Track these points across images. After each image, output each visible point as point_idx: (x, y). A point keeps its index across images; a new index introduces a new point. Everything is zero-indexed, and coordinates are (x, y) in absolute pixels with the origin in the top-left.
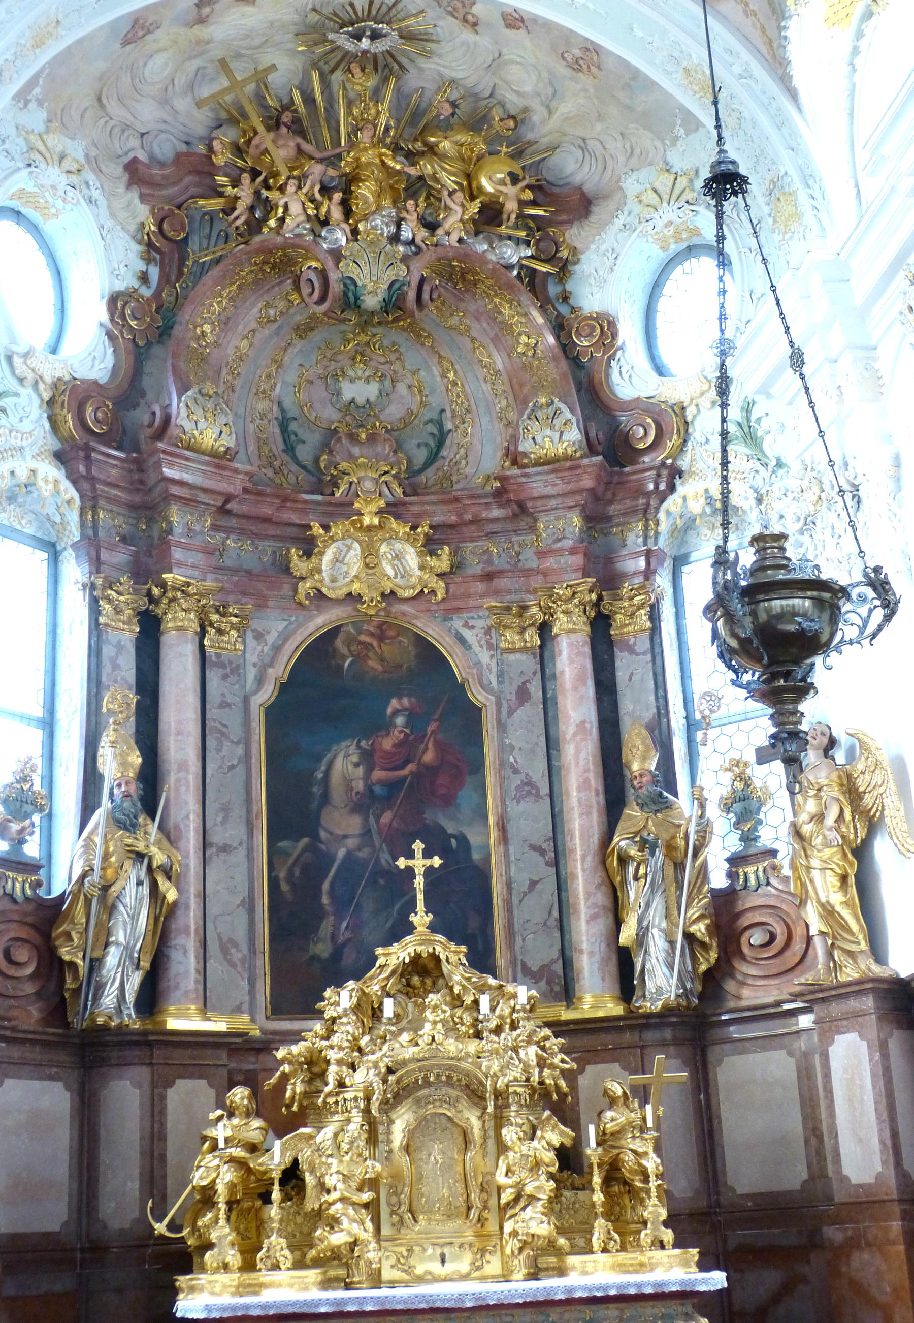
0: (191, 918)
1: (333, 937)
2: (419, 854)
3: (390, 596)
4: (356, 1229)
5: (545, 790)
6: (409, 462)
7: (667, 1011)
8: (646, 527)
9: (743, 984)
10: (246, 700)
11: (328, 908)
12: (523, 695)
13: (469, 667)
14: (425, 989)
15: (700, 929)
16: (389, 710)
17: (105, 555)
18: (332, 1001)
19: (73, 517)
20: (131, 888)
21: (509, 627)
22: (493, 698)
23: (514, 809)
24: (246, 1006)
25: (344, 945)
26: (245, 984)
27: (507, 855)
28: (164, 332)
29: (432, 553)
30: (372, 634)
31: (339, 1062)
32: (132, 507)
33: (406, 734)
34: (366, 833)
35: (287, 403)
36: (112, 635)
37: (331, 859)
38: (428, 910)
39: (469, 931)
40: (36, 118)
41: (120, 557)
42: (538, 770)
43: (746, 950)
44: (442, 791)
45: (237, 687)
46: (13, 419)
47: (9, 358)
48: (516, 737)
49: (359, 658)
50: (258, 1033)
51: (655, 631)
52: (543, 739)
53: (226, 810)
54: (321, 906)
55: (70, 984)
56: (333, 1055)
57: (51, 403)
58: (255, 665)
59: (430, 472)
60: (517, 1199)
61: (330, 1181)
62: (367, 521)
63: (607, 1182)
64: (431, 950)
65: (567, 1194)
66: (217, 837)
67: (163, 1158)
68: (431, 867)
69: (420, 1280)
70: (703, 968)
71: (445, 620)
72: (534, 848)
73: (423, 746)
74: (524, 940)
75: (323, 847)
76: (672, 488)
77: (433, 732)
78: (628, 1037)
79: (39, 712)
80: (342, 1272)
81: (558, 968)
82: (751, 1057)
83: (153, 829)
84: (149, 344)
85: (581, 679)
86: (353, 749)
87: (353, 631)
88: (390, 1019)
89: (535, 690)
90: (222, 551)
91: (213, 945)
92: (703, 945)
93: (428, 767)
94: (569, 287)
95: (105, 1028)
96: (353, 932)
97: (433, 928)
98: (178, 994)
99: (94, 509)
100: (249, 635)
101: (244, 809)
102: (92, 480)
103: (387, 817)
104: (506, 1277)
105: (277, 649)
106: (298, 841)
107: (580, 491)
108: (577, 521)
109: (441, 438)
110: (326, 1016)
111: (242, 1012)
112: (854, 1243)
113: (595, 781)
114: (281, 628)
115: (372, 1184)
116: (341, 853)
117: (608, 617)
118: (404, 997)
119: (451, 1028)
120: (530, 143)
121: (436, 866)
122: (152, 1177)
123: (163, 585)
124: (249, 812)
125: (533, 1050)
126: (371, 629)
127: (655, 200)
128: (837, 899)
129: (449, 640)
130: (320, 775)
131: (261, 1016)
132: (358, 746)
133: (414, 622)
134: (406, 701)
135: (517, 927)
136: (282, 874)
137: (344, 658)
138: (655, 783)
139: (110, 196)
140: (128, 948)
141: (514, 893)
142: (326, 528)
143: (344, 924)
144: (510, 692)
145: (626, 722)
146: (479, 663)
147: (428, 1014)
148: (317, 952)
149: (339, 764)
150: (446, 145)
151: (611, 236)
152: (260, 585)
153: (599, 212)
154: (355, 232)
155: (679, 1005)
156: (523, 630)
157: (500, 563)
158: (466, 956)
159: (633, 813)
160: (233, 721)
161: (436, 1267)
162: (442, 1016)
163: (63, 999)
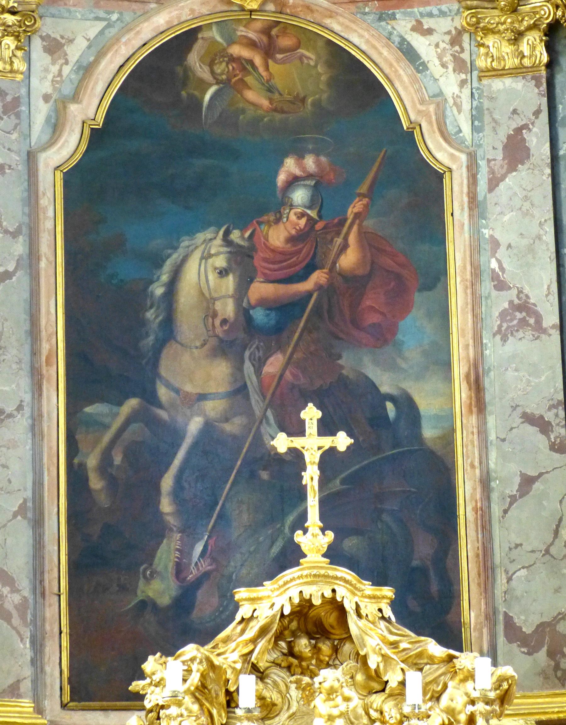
2: (312, 428)
11: (171, 520)
13: (422, 102)
14: (319, 661)
16: (282, 178)
18: (156, 678)
21: (493, 32)
22: (463, 157)
24: (26, 686)
25: (198, 583)
27: (482, 432)
30: (252, 44)
33: (310, 218)
39: (415, 563)
44: (372, 319)
45: (14, 136)
52: (550, 228)
54: (158, 514)
58: (46, 98)
64: (328, 594)
68: (332, 450)
71: (380, 19)
73: (339, 241)
74: (509, 580)
75: (163, 415)
77: (357, 216)
86: (217, 245)
87: (219, 38)
88: (249, 711)
96: (214, 560)
100: (37, 44)
101: (27, 348)
106: (120, 404)
110: (148, 704)
111: (19, 696)
114: (92, 33)
118: (283, 674)
121: (342, 448)
124: (35, 353)
126: (252, 35)
130: (159, 290)
133: (328, 22)
134: (310, 162)
135: (498, 556)
136: (92, 462)
137: (203, 86)
141: (495, 496)
143: (199, 548)
146: (440, 94)
147: (319, 702)
148: (151, 594)
156: (518, 36)
158: (393, 604)
162: (343, 707)
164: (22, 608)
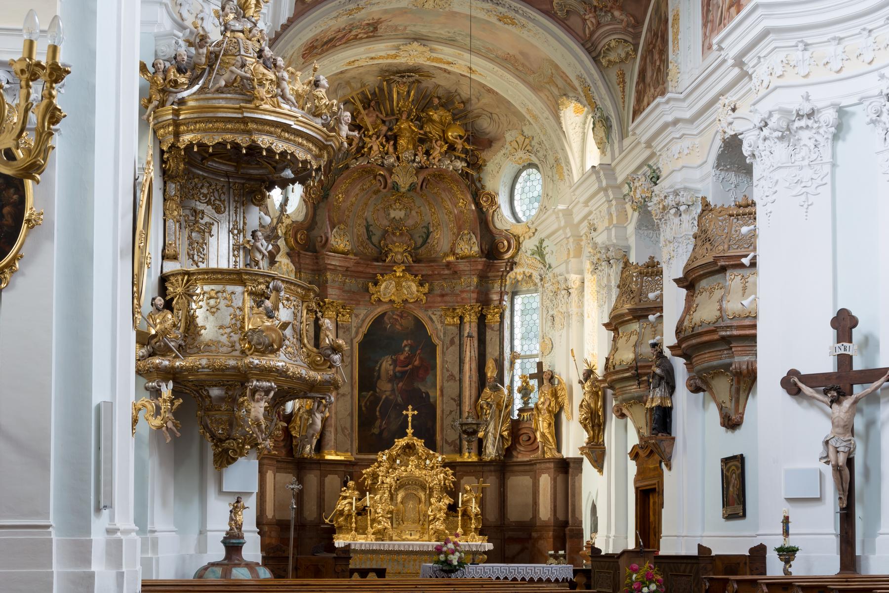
1: (380, 427)
2: (410, 410)
3: (405, 301)
5: (458, 378)
6: (415, 243)
7: (491, 461)
8: (502, 282)
9: (519, 453)
10: (352, 340)
12: (452, 342)
15: (505, 433)
16: (403, 345)
23: (446, 384)
28: (325, 197)
30: (398, 315)
31: (382, 476)
32: (313, 270)
34: (393, 390)
35: (369, 220)
37: (379, 399)
38: (413, 427)
42: (456, 371)
43: (521, 441)
48: (449, 358)
49: (393, 325)
50: (353, 459)
51: (502, 322)
56: (380, 474)
59: (423, 248)
60: (434, 519)
61: (379, 511)
62: (398, 274)
63: (463, 515)
65: (451, 518)
67: (324, 500)
69: (404, 540)
70: (506, 447)
72: (452, 399)
76: (512, 269)
78: (478, 468)
80: (381, 536)
81: (458, 442)
82: (519, 478)
84: (319, 203)
86: (389, 359)
89: (457, 340)
90: (344, 283)
92: (507, 439)
94: (482, 176)
95: (306, 458)
97: (414, 434)
98: (328, 446)
99: (300, 272)
103: (400, 385)
104: (430, 541)
105: (363, 321)
107: (478, 270)
108: (475, 280)
109: (428, 234)
112: (540, 538)
113: (475, 378)
115: (391, 512)
116: (384, 397)
117: (485, 316)
119: (417, 466)
122: (320, 506)
123: (324, 302)
125: (442, 475)
127: (516, 147)
128: (546, 431)
129: (426, 319)
130: (377, 368)
131: (354, 453)
132: (391, 358)
134: (409, 342)
135: (445, 426)
136: (363, 404)
138: (495, 381)
142: (383, 277)
145: (488, 356)
149: (384, 364)
150: (436, 117)
151: (500, 155)
153: (495, 146)
154: (398, 158)
155: (496, 459)
156: (453, 317)
157: (447, 290)
159: (487, 390)
161: (409, 537)
163: (292, 448)
164: (349, 434)
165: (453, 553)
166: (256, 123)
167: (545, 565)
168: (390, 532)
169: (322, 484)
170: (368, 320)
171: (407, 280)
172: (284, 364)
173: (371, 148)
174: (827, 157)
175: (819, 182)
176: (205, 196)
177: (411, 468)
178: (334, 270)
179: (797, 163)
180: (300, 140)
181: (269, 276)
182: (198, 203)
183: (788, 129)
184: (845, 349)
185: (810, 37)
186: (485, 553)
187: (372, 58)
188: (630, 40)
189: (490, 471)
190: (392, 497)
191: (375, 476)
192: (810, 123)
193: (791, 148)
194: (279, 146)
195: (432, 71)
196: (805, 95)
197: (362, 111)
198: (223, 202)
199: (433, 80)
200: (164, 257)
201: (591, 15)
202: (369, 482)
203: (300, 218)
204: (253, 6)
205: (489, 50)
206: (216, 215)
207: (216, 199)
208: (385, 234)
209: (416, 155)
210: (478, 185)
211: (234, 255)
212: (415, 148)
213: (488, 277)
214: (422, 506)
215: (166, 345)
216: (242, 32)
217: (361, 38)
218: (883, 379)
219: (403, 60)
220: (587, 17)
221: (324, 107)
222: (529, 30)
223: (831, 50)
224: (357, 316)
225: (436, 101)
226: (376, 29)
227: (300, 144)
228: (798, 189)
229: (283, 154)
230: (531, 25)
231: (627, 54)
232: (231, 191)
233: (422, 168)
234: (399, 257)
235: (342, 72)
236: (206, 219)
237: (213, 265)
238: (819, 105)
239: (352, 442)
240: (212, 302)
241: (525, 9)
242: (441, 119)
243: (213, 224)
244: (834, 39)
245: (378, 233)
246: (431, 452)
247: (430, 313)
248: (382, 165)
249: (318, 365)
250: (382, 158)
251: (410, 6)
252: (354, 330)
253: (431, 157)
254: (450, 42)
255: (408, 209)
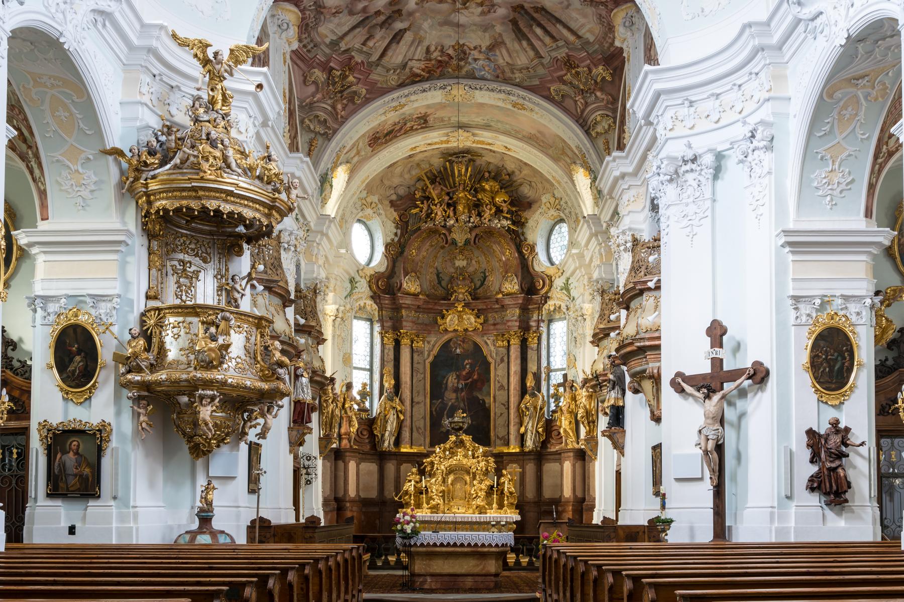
0: (408, 422)
3: (466, 330)
4: (439, 501)
5: (506, 388)
6: (475, 285)
7: (530, 452)
8: (539, 313)
12: (502, 360)
15: (540, 430)
17: (385, 324)
19: (376, 313)
20: (392, 416)
26: (423, 439)
28: (402, 253)
29: (478, 317)
32: (392, 309)
34: (457, 398)
35: (439, 268)
36: (387, 346)
37: (447, 405)
40: (364, 194)
41: (388, 324)
46: (359, 289)
47: (358, 271)
48: (500, 372)
51: (539, 343)
53: (418, 392)
55: (377, 440)
57: (369, 282)
66: (416, 400)
76: (546, 302)
78: (520, 457)
79: (368, 367)
81: (507, 437)
82: (552, 464)
83: (397, 400)
84: (397, 257)
85: (516, 358)
89: (506, 359)
90: (418, 318)
91: (414, 429)
93: (475, 380)
95: (385, 451)
98: (404, 442)
99: (382, 310)
102: (381, 304)
105: (434, 346)
108: (517, 311)
109: (485, 278)
113: (518, 388)
115: (443, 491)
116: (450, 404)
119: (466, 456)
120: (514, 182)
123: (400, 332)
125: (483, 463)
127: (549, 206)
129: (483, 343)
131: (427, 447)
138: (533, 389)
139: (385, 210)
140: (391, 432)
144: (498, 360)
149: (450, 378)
150: (487, 187)
152: (429, 328)
153: (534, 207)
154: (457, 220)
155: (533, 450)
156: (503, 341)
157: (498, 320)
159: (527, 397)
160: (421, 367)
161: (457, 511)
165: (408, 523)
166: (204, 191)
167: (487, 533)
168: (442, 507)
169: (398, 471)
170: (437, 346)
171: (467, 313)
172: (223, 377)
173: (436, 214)
174: (708, 194)
175: (702, 215)
176: (193, 250)
177: (460, 458)
178: (408, 308)
179: (684, 201)
180: (246, 202)
181: (218, 309)
182: (186, 255)
183: (676, 172)
184: (716, 354)
185: (693, 95)
186: (514, 523)
187: (429, 144)
188: (610, 114)
189: (530, 459)
190: (444, 481)
191: (432, 463)
192: (694, 166)
193: (679, 189)
194: (226, 208)
195: (484, 152)
196: (687, 143)
197: (429, 186)
198: (209, 254)
199: (484, 158)
200: (148, 297)
201: (580, 97)
202: (428, 469)
203: (382, 269)
204: (220, 101)
205: (517, 132)
206: (203, 264)
207: (203, 252)
208: (452, 279)
209: (470, 217)
210: (522, 238)
211: (218, 295)
212: (470, 212)
213: (529, 309)
214: (467, 487)
215: (138, 365)
216: (209, 121)
217: (417, 129)
218: (743, 378)
219: (455, 144)
220: (577, 99)
221: (273, 176)
222: (537, 113)
223: (711, 104)
224: (429, 342)
225: (487, 175)
226: (426, 121)
227: (246, 206)
228: (685, 222)
229: (231, 213)
230: (536, 109)
231: (609, 125)
232: (216, 245)
233: (475, 227)
234: (461, 296)
235: (410, 156)
236: (193, 268)
237: (200, 301)
238: (700, 151)
239: (425, 438)
240: (175, 330)
241: (530, 96)
242: (491, 189)
243: (200, 271)
244: (712, 95)
245: (446, 279)
246: (477, 445)
247: (485, 338)
248: (444, 226)
249: (268, 377)
250: (445, 220)
251: (444, 101)
252: (426, 353)
253: (483, 218)
254: (487, 127)
255: (469, 259)
